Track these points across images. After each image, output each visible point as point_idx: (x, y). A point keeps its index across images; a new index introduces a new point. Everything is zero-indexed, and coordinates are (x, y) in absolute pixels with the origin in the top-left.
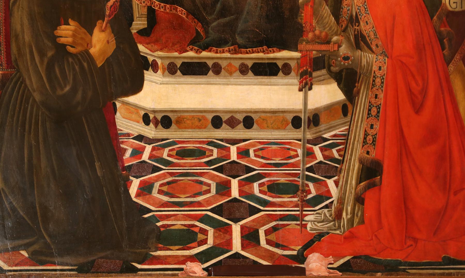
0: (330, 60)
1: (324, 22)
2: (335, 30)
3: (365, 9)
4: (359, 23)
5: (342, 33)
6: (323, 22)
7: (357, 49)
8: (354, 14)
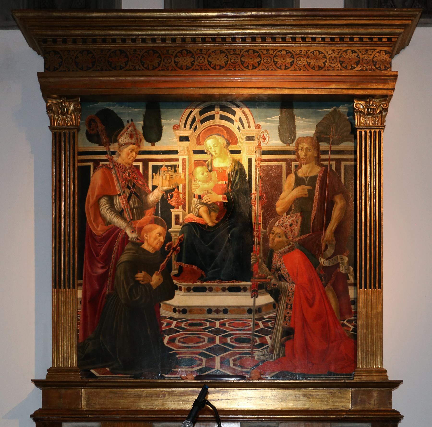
8: (278, 267)
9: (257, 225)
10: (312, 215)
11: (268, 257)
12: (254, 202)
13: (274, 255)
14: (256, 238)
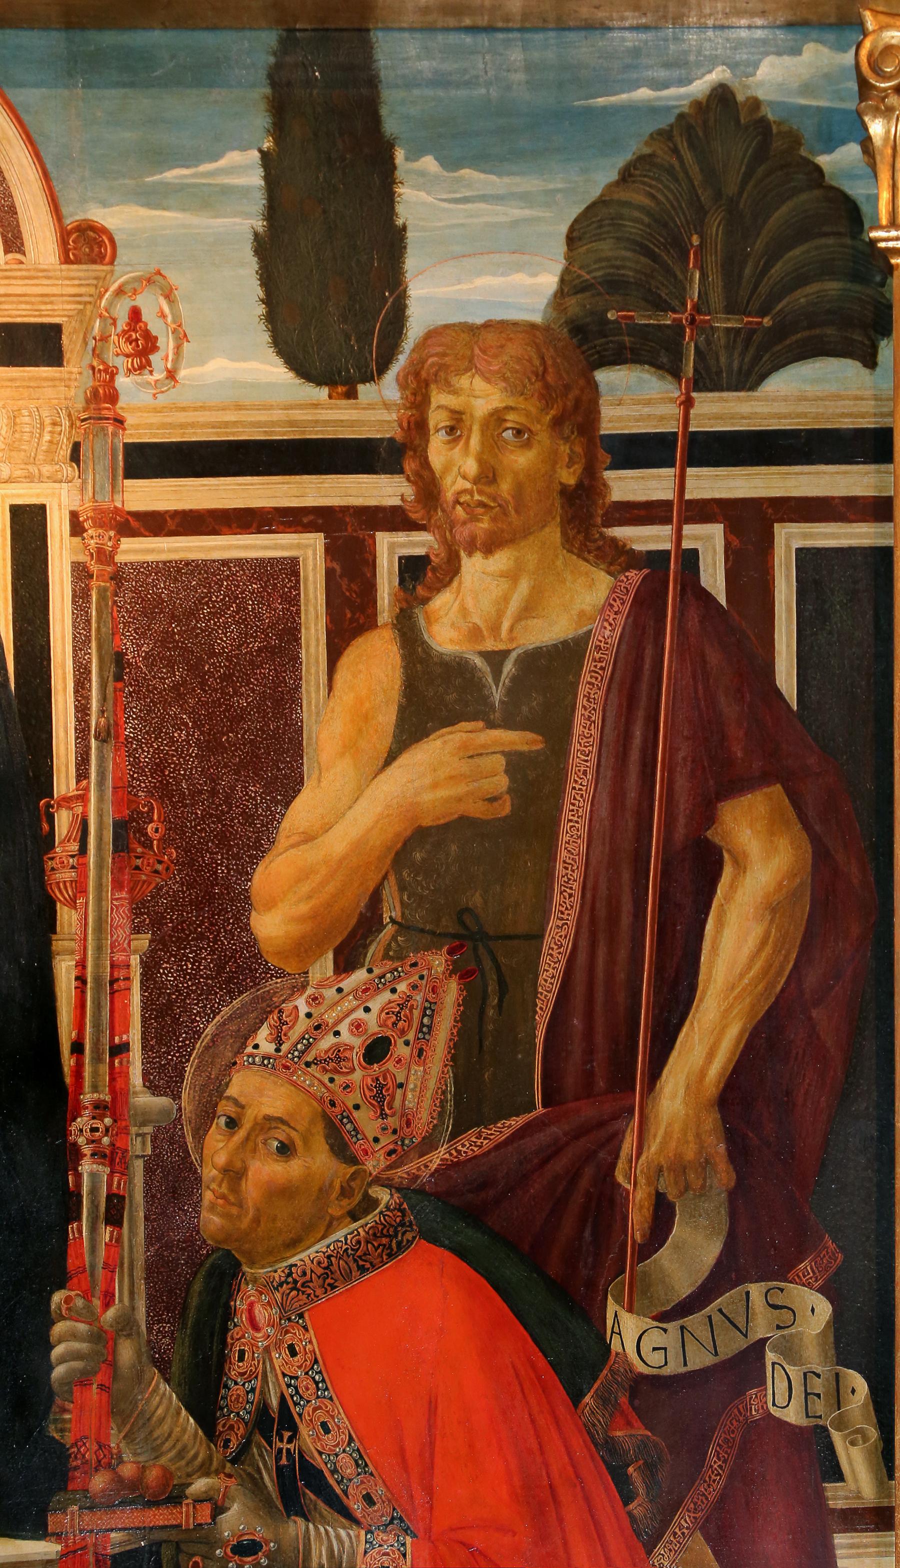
0: (182, 1558)
1: (155, 1435)
2: (200, 1459)
3: (317, 1383)
4: (294, 1429)
5: (228, 1465)
6: (151, 1432)
7: (289, 1516)
8: (274, 1402)
9: (97, 1059)
10: (545, 960)
11: (192, 1314)
12: (67, 875)
13: (240, 1304)
14: (86, 1167)
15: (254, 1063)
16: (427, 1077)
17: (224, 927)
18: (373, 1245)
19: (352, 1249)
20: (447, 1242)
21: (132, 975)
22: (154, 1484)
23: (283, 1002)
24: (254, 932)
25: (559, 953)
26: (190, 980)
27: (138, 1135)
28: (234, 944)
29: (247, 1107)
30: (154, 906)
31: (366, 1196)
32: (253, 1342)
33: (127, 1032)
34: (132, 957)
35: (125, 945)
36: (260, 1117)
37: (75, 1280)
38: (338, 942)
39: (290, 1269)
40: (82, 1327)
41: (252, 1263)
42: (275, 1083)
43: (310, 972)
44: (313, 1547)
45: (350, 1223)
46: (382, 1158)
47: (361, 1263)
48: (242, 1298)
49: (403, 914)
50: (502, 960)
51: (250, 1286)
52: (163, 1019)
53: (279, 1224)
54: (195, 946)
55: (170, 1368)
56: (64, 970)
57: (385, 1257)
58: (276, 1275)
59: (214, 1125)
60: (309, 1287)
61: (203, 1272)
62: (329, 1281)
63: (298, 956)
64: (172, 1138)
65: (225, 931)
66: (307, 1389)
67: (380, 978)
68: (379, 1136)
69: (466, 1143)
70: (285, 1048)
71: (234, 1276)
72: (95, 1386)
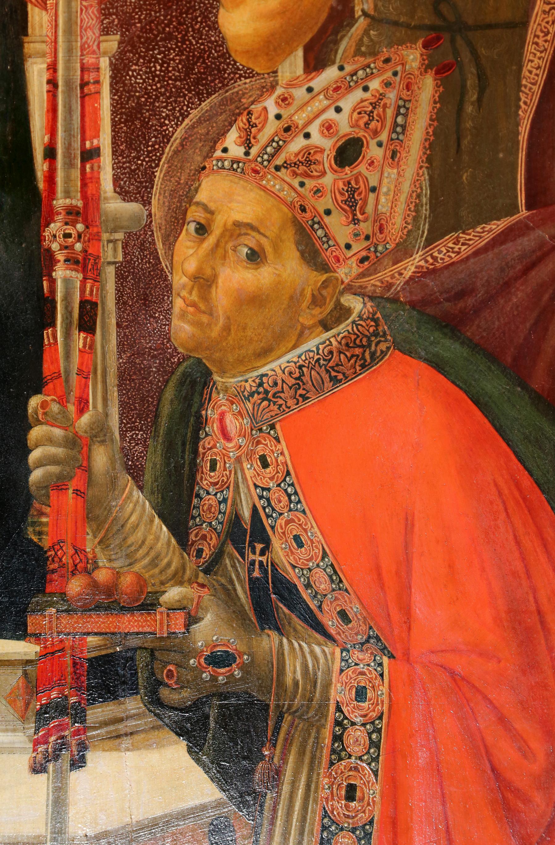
0: (157, 665)
1: (130, 541)
2: (173, 567)
3: (289, 496)
4: (267, 543)
5: (201, 575)
6: (125, 539)
7: (263, 629)
8: (246, 514)
9: (69, 165)
10: (530, 48)
11: (164, 422)
13: (211, 413)
15: (223, 168)
16: (401, 180)
17: (192, 26)
18: (346, 356)
19: (324, 360)
20: (423, 353)
21: (102, 79)
22: (128, 591)
23: (253, 103)
24: (222, 31)
25: (546, 41)
26: (159, 82)
27: (109, 241)
28: (202, 44)
29: (216, 213)
30: (122, 6)
31: (339, 306)
32: (224, 452)
33: (97, 136)
34: (102, 59)
35: (95, 47)
36: (230, 223)
37: (51, 386)
38: (307, 39)
39: (261, 379)
40: (58, 432)
41: (223, 372)
42: (245, 188)
43: (280, 71)
44: (287, 662)
45: (321, 333)
46: (354, 265)
47: (333, 374)
48: (213, 407)
49: (376, 6)
50: (482, 51)
51: (221, 395)
52: (133, 123)
53: (249, 333)
54: (164, 46)
55: (143, 475)
56: (36, 73)
57: (358, 368)
58: (247, 385)
59: (184, 232)
60: (281, 398)
61: (175, 379)
62: (301, 392)
63: (267, 54)
64: (142, 245)
65: (193, 30)
66: (280, 501)
67: (352, 76)
68: (351, 243)
69: (444, 250)
70: (254, 151)
71: (205, 384)
72: (71, 491)
